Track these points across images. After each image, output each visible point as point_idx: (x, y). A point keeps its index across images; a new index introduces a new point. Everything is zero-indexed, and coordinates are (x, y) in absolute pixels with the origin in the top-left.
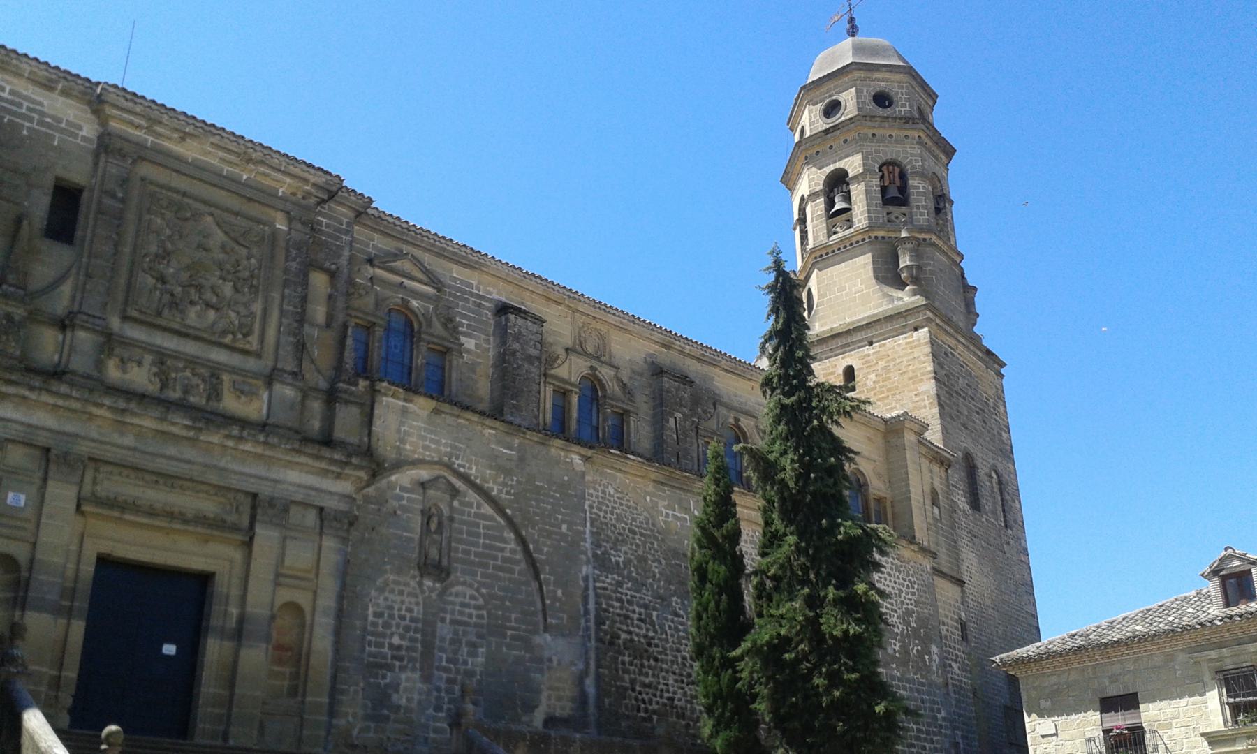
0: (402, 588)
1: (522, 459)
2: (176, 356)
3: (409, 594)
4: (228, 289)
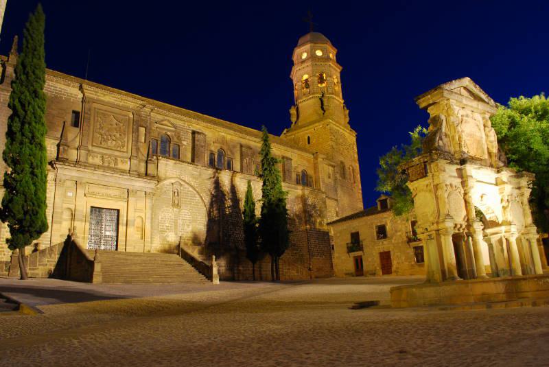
1: (200, 175)
2: (106, 154)
4: (118, 135)
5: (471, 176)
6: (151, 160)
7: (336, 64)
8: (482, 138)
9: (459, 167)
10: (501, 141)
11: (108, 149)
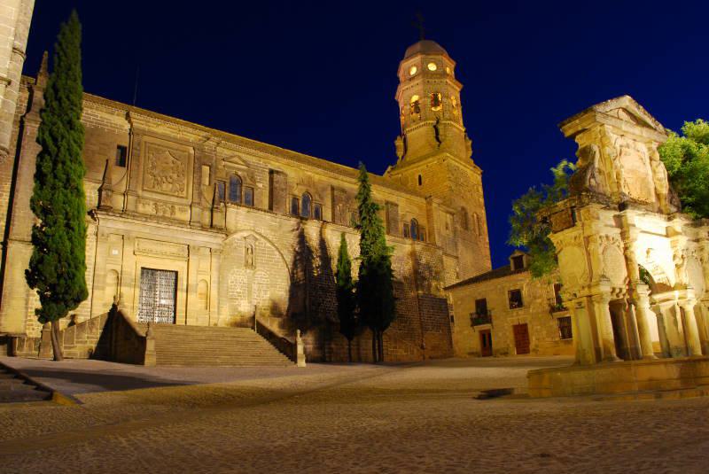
4: (175, 176)
5: (634, 226)
6: (217, 208)
7: (454, 81)
8: (647, 174)
9: (617, 213)
10: (672, 179)
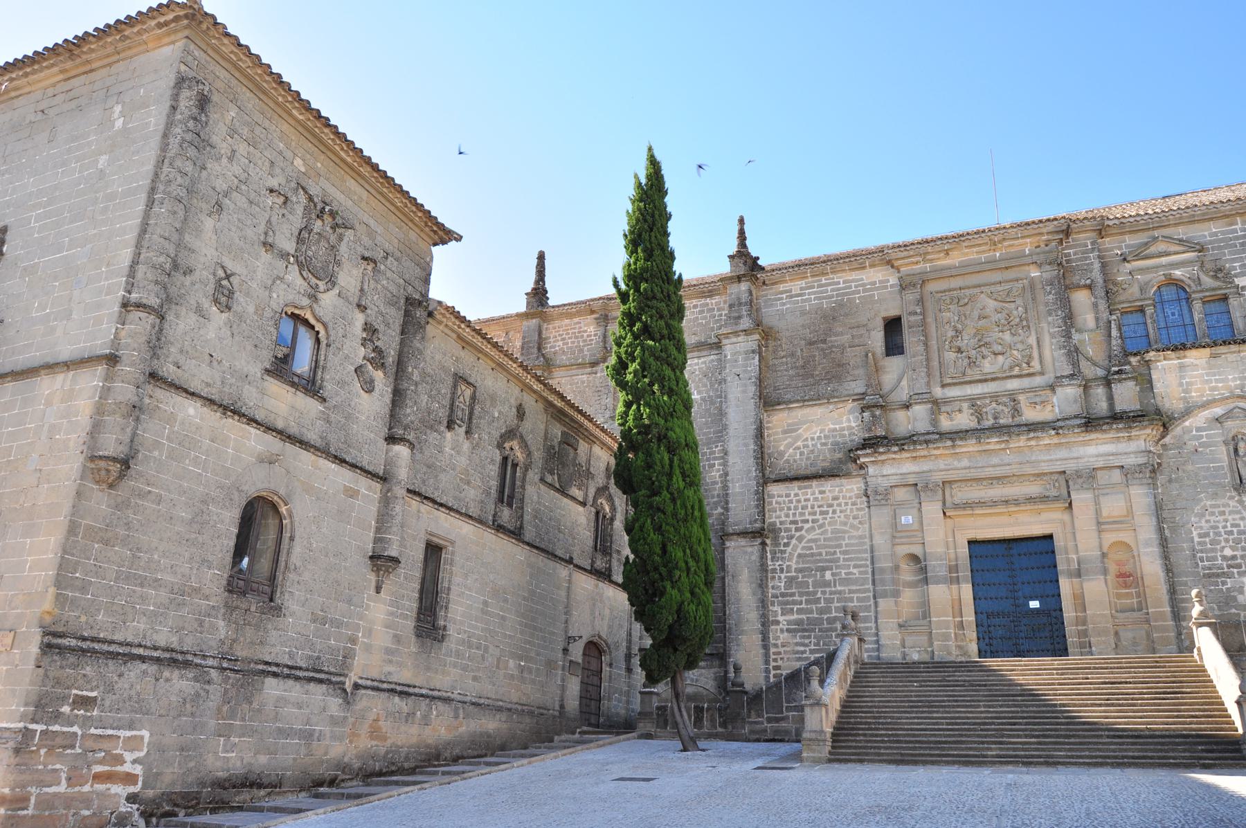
0: (1222, 509)
3: (1231, 513)
4: (1007, 337)
11: (986, 380)
